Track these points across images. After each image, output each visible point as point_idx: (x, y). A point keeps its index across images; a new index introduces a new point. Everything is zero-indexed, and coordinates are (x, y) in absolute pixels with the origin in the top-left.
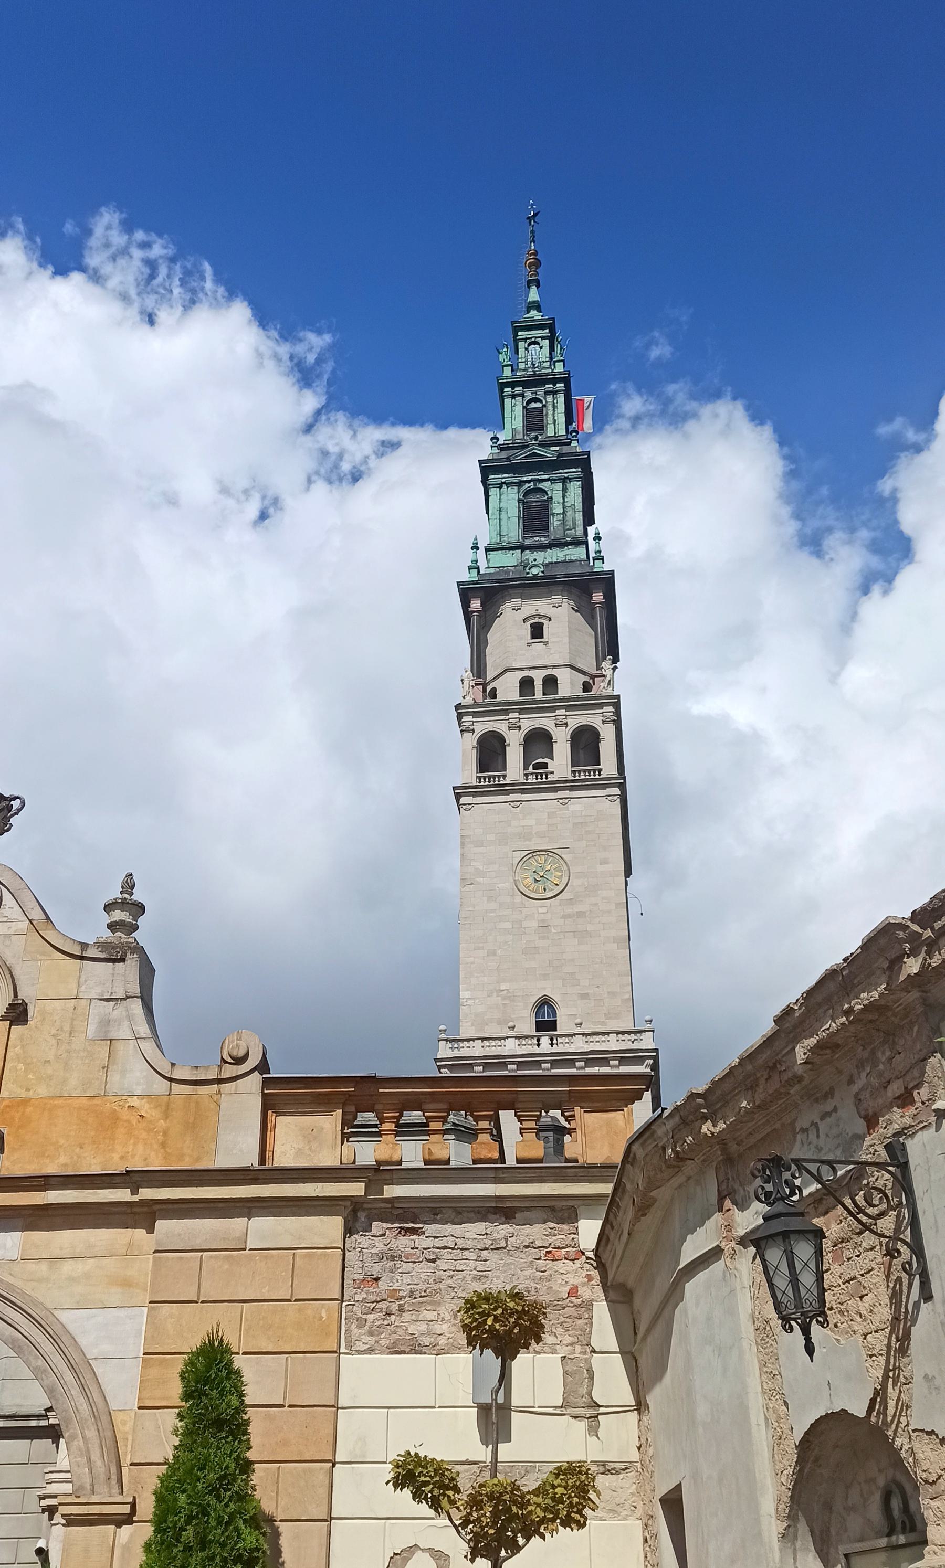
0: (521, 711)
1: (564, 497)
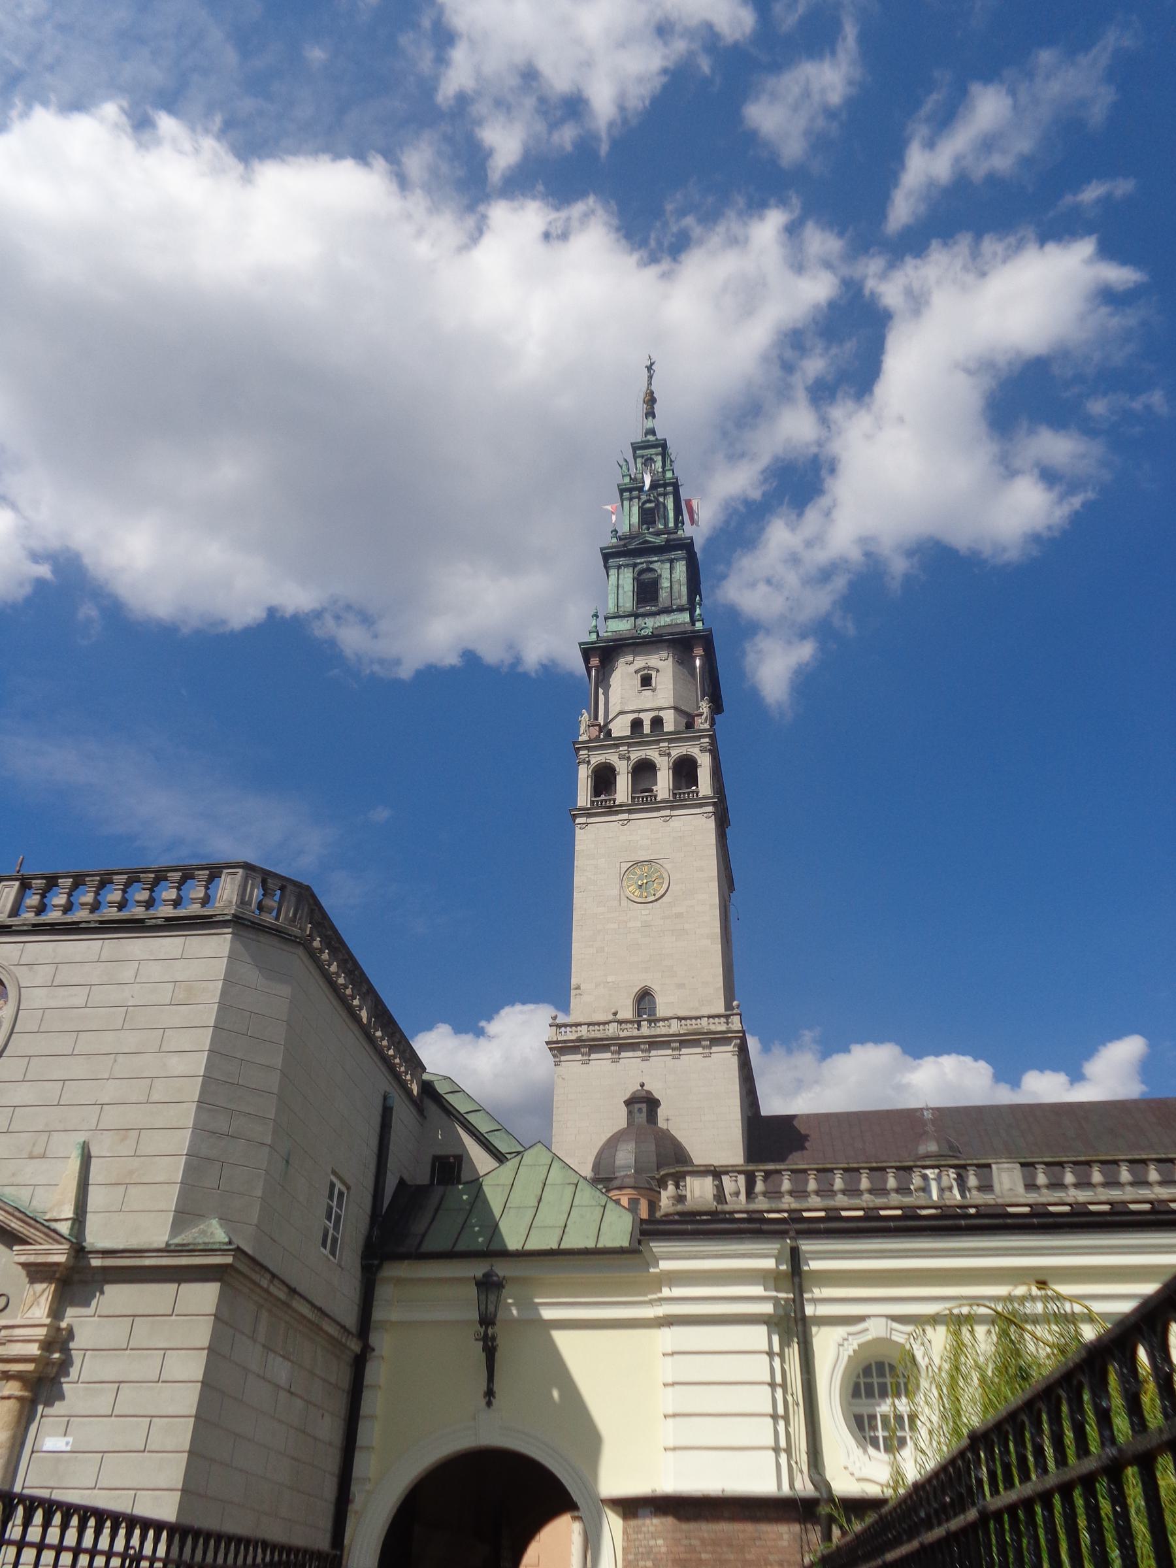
0: (629, 745)
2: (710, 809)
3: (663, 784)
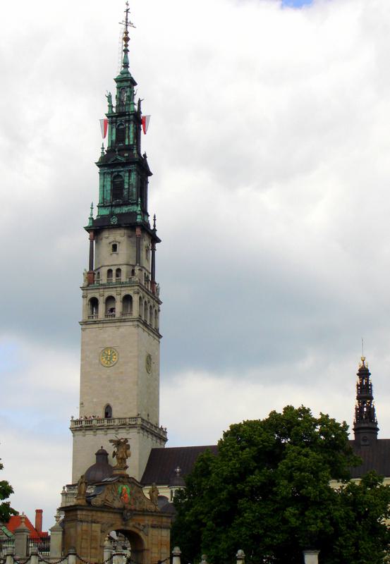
1: (129, 180)
2: (136, 323)
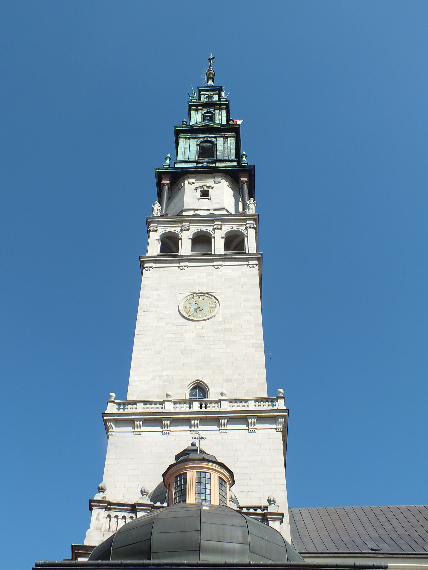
2: (256, 262)
3: (219, 246)
